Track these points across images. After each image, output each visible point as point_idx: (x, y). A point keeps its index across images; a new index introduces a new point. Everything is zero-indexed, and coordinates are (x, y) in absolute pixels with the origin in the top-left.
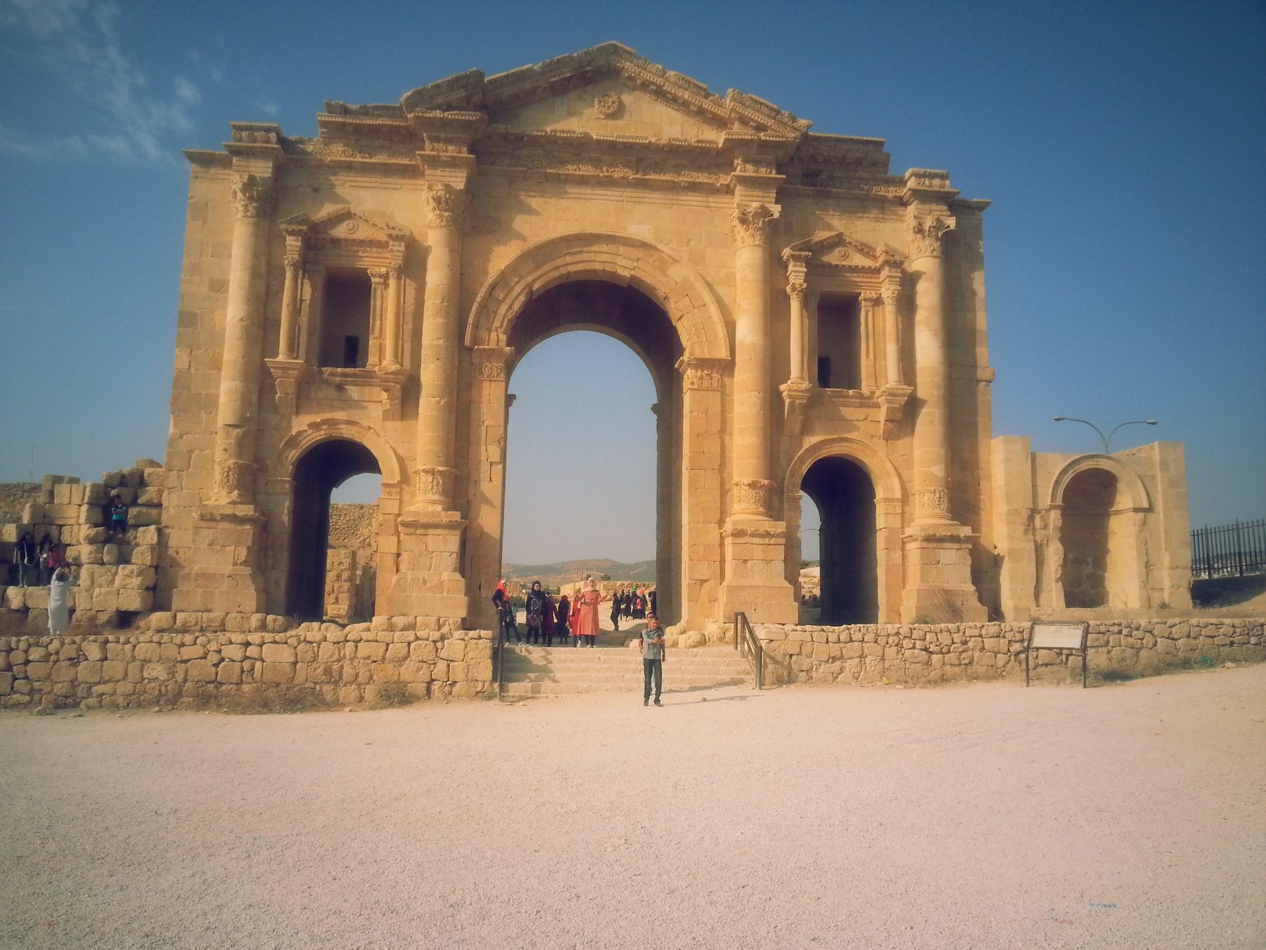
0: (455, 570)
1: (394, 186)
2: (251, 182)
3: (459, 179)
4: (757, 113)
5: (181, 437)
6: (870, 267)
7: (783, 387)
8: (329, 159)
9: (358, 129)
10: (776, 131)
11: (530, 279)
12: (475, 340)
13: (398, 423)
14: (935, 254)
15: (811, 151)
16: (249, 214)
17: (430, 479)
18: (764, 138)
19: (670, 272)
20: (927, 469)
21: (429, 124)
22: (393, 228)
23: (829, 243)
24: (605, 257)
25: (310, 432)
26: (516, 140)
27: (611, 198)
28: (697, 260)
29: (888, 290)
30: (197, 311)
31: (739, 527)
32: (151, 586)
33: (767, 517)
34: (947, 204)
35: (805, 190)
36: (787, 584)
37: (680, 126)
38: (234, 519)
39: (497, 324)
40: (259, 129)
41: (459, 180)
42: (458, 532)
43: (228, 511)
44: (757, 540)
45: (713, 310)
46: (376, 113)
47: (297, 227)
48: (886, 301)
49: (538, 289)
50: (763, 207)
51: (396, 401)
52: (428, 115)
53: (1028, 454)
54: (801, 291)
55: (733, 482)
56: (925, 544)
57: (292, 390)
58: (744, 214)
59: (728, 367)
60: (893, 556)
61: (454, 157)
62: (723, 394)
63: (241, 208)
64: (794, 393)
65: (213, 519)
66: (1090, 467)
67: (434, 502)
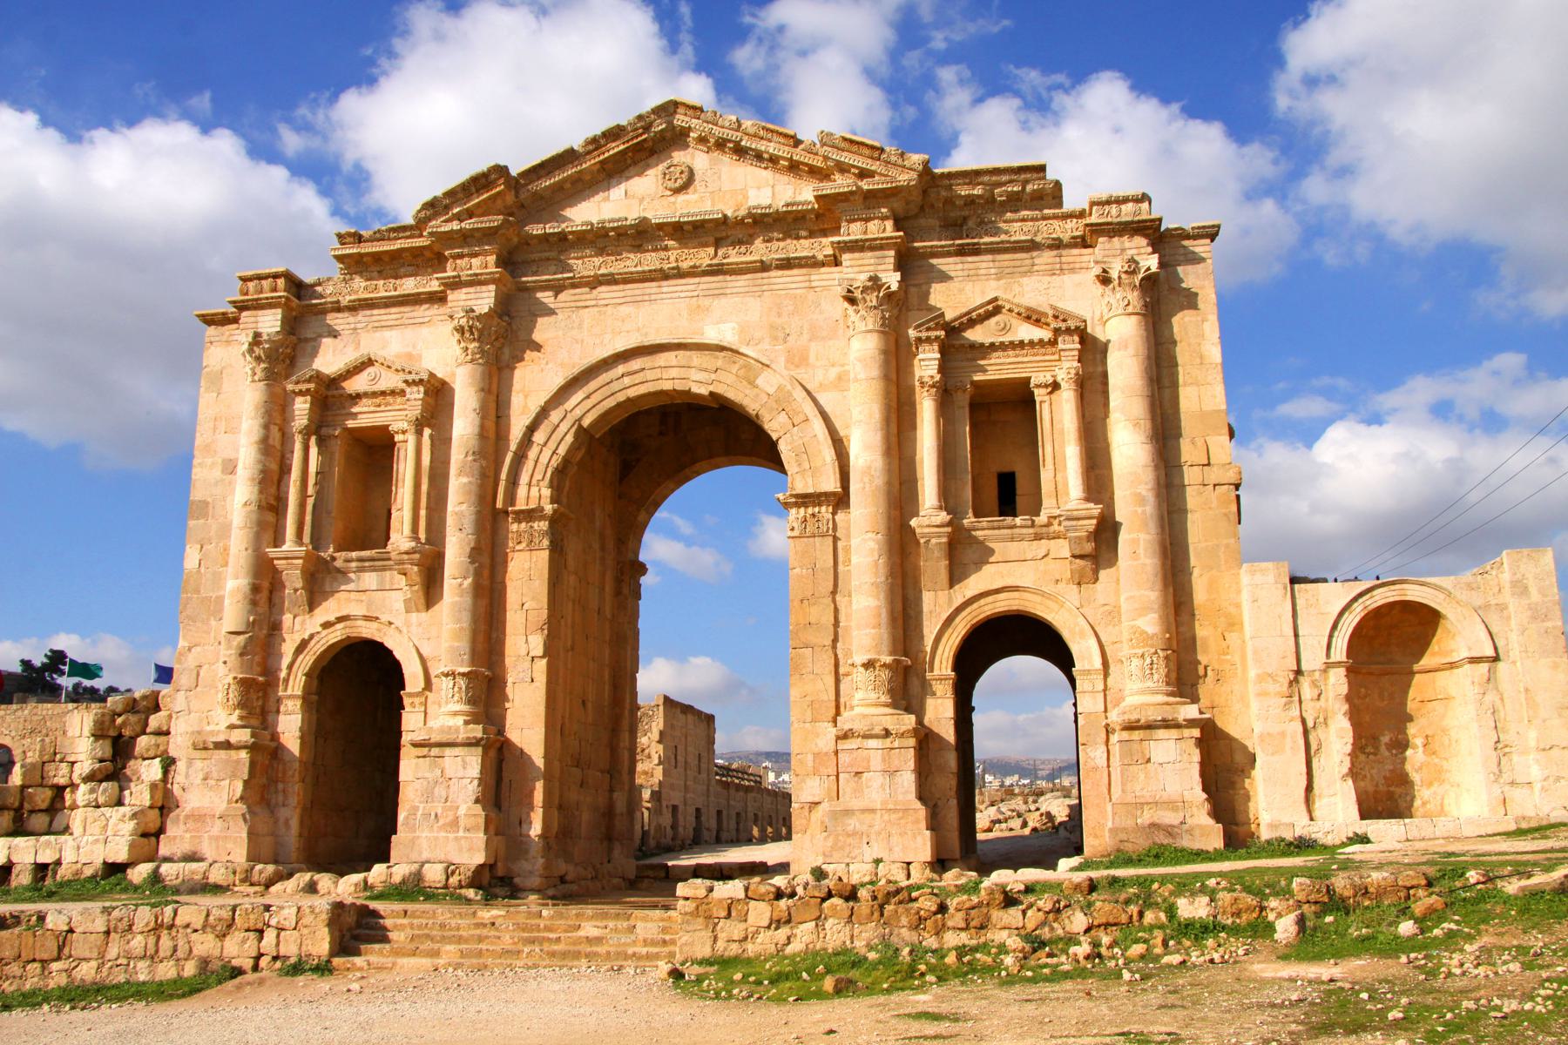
0: (477, 801)
1: (421, 320)
2: (257, 339)
3: (487, 301)
4: (860, 158)
5: (190, 649)
6: (1041, 341)
7: (913, 522)
8: (348, 298)
9: (377, 257)
10: (887, 176)
11: (578, 412)
12: (511, 497)
13: (424, 614)
14: (1130, 309)
15: (944, 193)
16: (256, 378)
17: (452, 683)
18: (866, 187)
19: (759, 382)
20: (1133, 623)
21: (448, 239)
22: (410, 373)
23: (980, 315)
24: (674, 373)
25: (325, 632)
26: (560, 240)
27: (682, 295)
28: (799, 359)
29: (1066, 368)
30: (209, 500)
31: (846, 727)
32: (153, 831)
33: (895, 708)
34: (1146, 236)
35: (942, 247)
36: (918, 805)
37: (770, 189)
38: (227, 745)
39: (538, 476)
40: (266, 277)
41: (484, 300)
42: (480, 750)
43: (221, 738)
44: (873, 743)
45: (818, 426)
46: (392, 235)
47: (304, 387)
48: (1063, 384)
49: (592, 425)
50: (874, 279)
51: (416, 588)
52: (442, 229)
53: (1285, 588)
54: (933, 386)
55: (850, 662)
56: (1125, 735)
57: (299, 584)
58: (849, 291)
59: (840, 500)
60: (1092, 755)
61: (476, 275)
62: (835, 539)
63: (250, 372)
64: (927, 530)
65: (205, 749)
66: (1391, 599)
67: (455, 714)
